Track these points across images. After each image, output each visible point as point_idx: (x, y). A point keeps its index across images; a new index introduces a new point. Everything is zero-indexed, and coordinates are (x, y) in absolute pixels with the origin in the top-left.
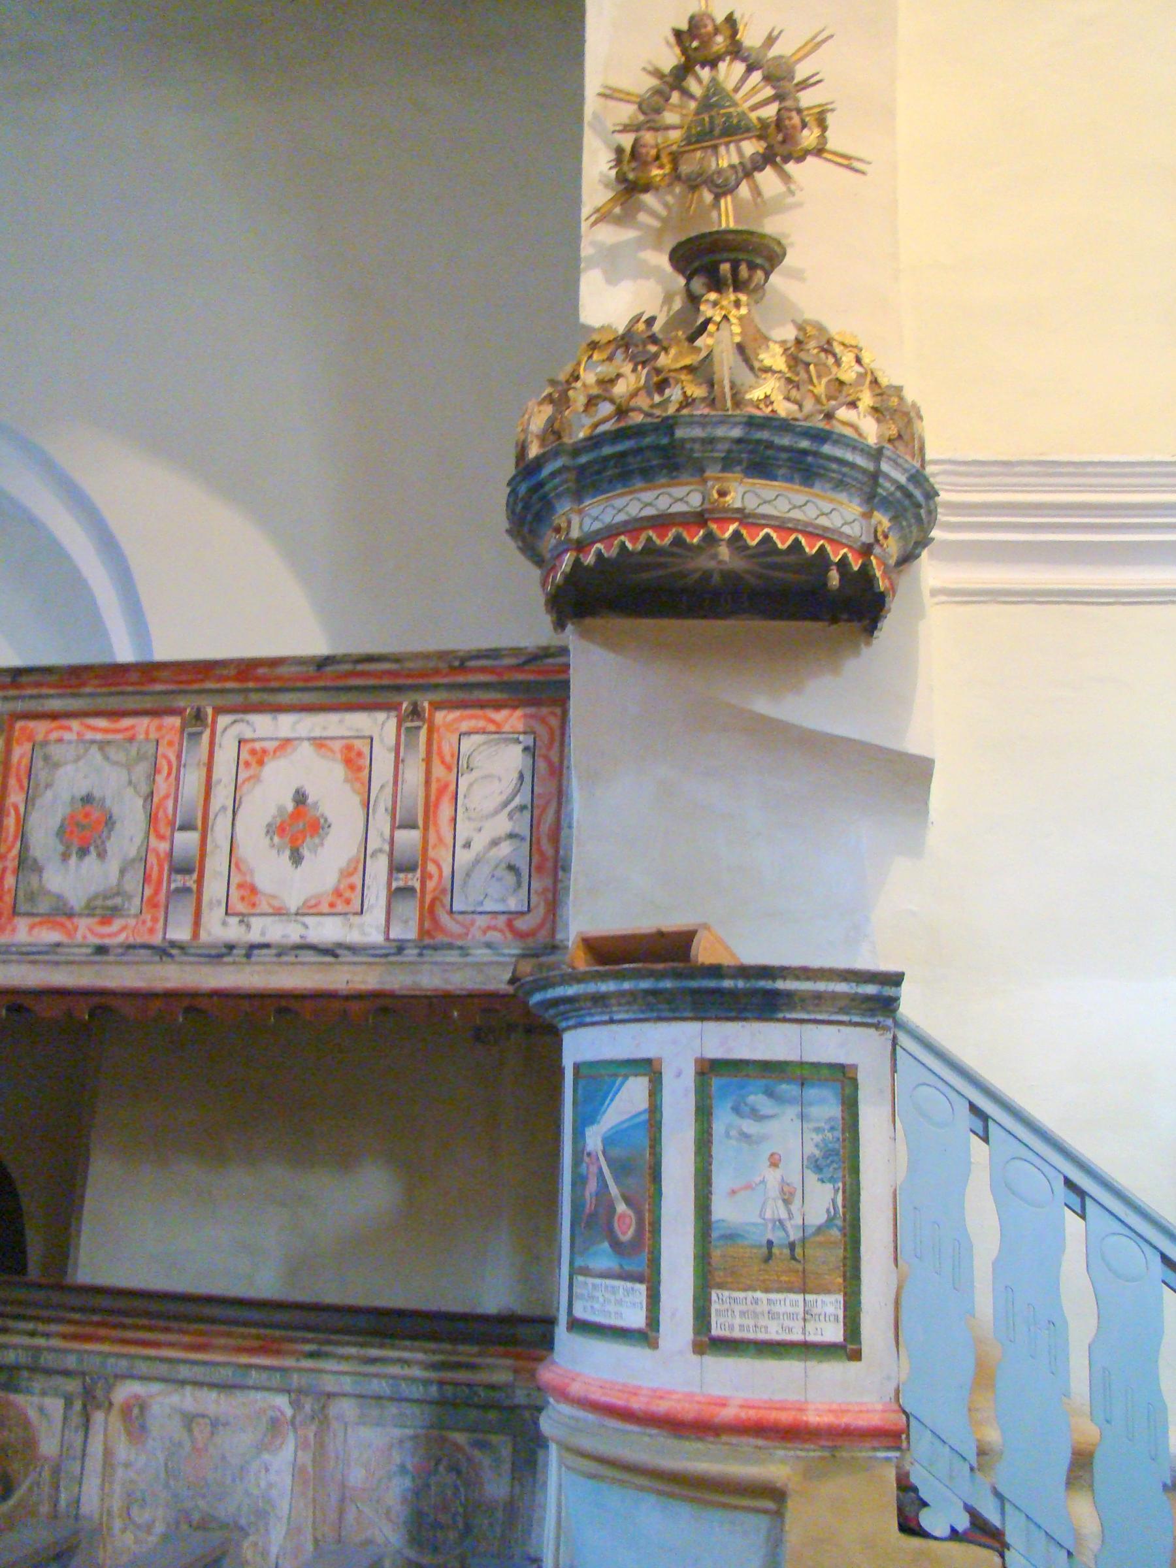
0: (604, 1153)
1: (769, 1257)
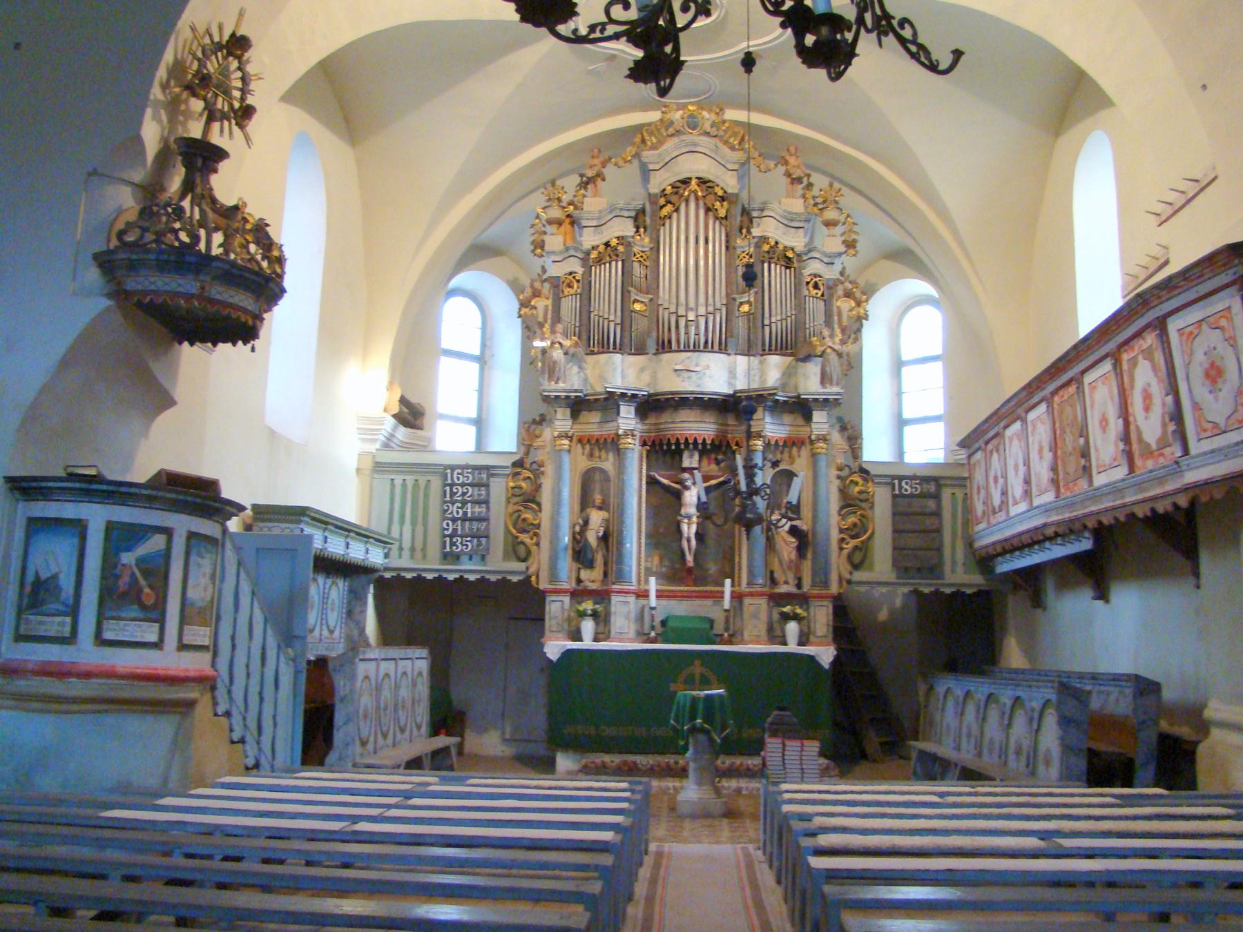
0: (137, 565)
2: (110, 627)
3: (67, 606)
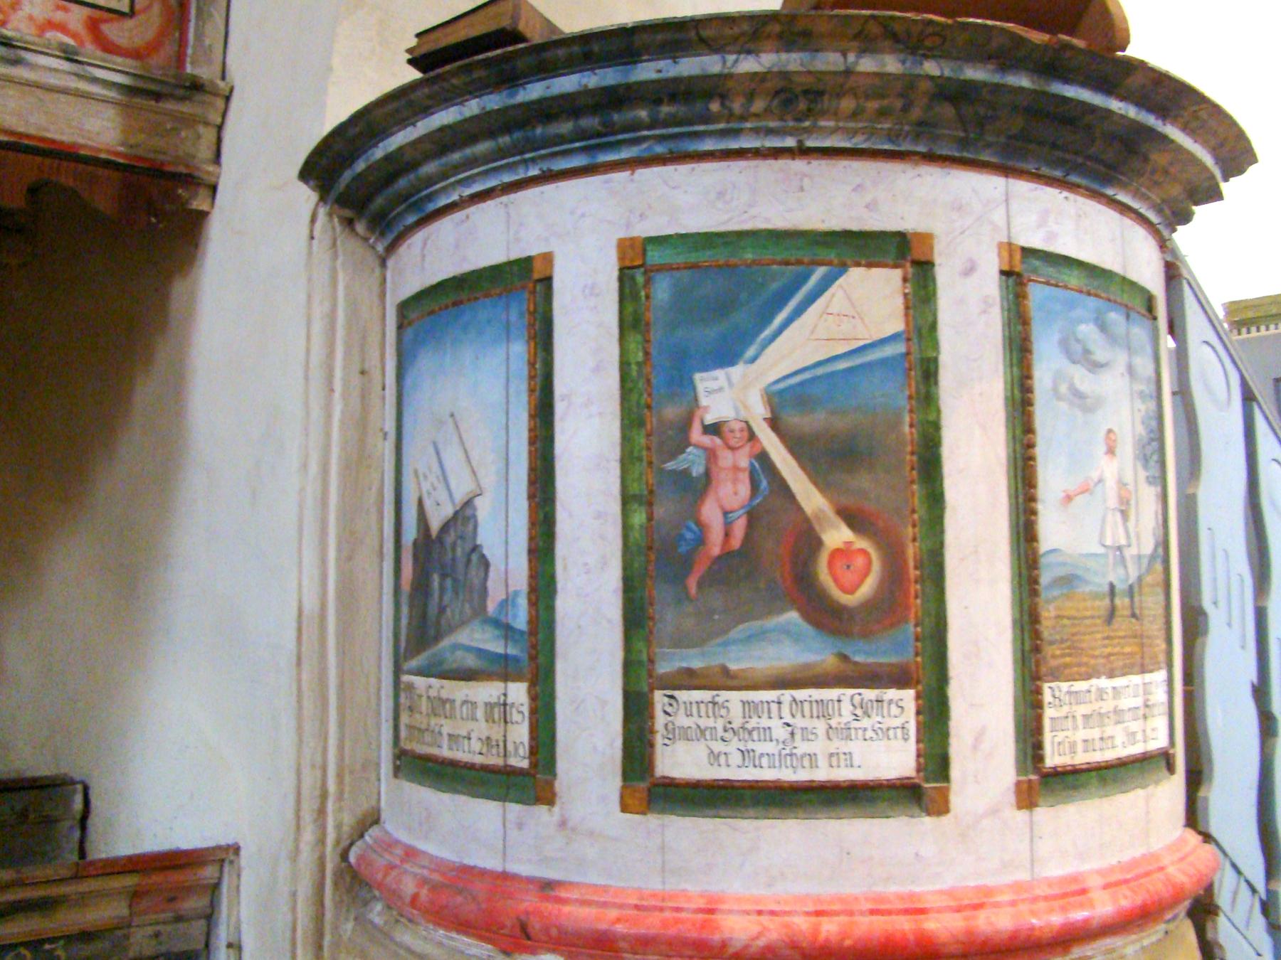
0: (774, 423)
1: (1112, 614)
2: (682, 720)
3: (507, 631)
